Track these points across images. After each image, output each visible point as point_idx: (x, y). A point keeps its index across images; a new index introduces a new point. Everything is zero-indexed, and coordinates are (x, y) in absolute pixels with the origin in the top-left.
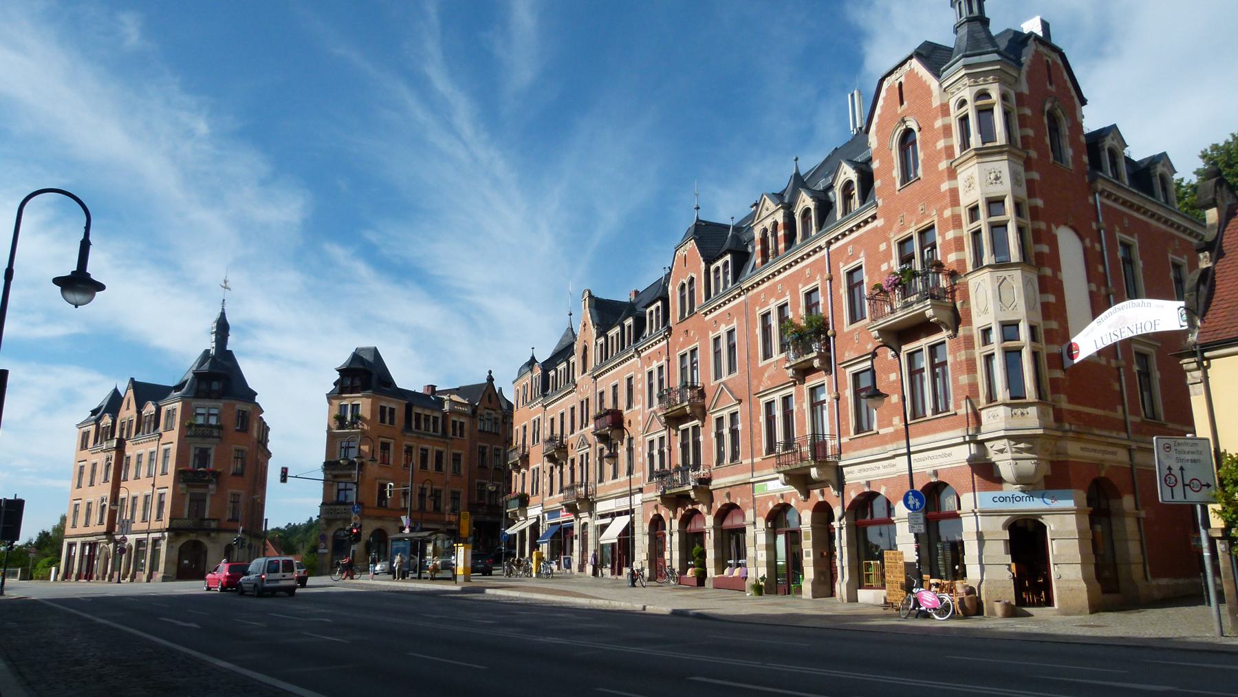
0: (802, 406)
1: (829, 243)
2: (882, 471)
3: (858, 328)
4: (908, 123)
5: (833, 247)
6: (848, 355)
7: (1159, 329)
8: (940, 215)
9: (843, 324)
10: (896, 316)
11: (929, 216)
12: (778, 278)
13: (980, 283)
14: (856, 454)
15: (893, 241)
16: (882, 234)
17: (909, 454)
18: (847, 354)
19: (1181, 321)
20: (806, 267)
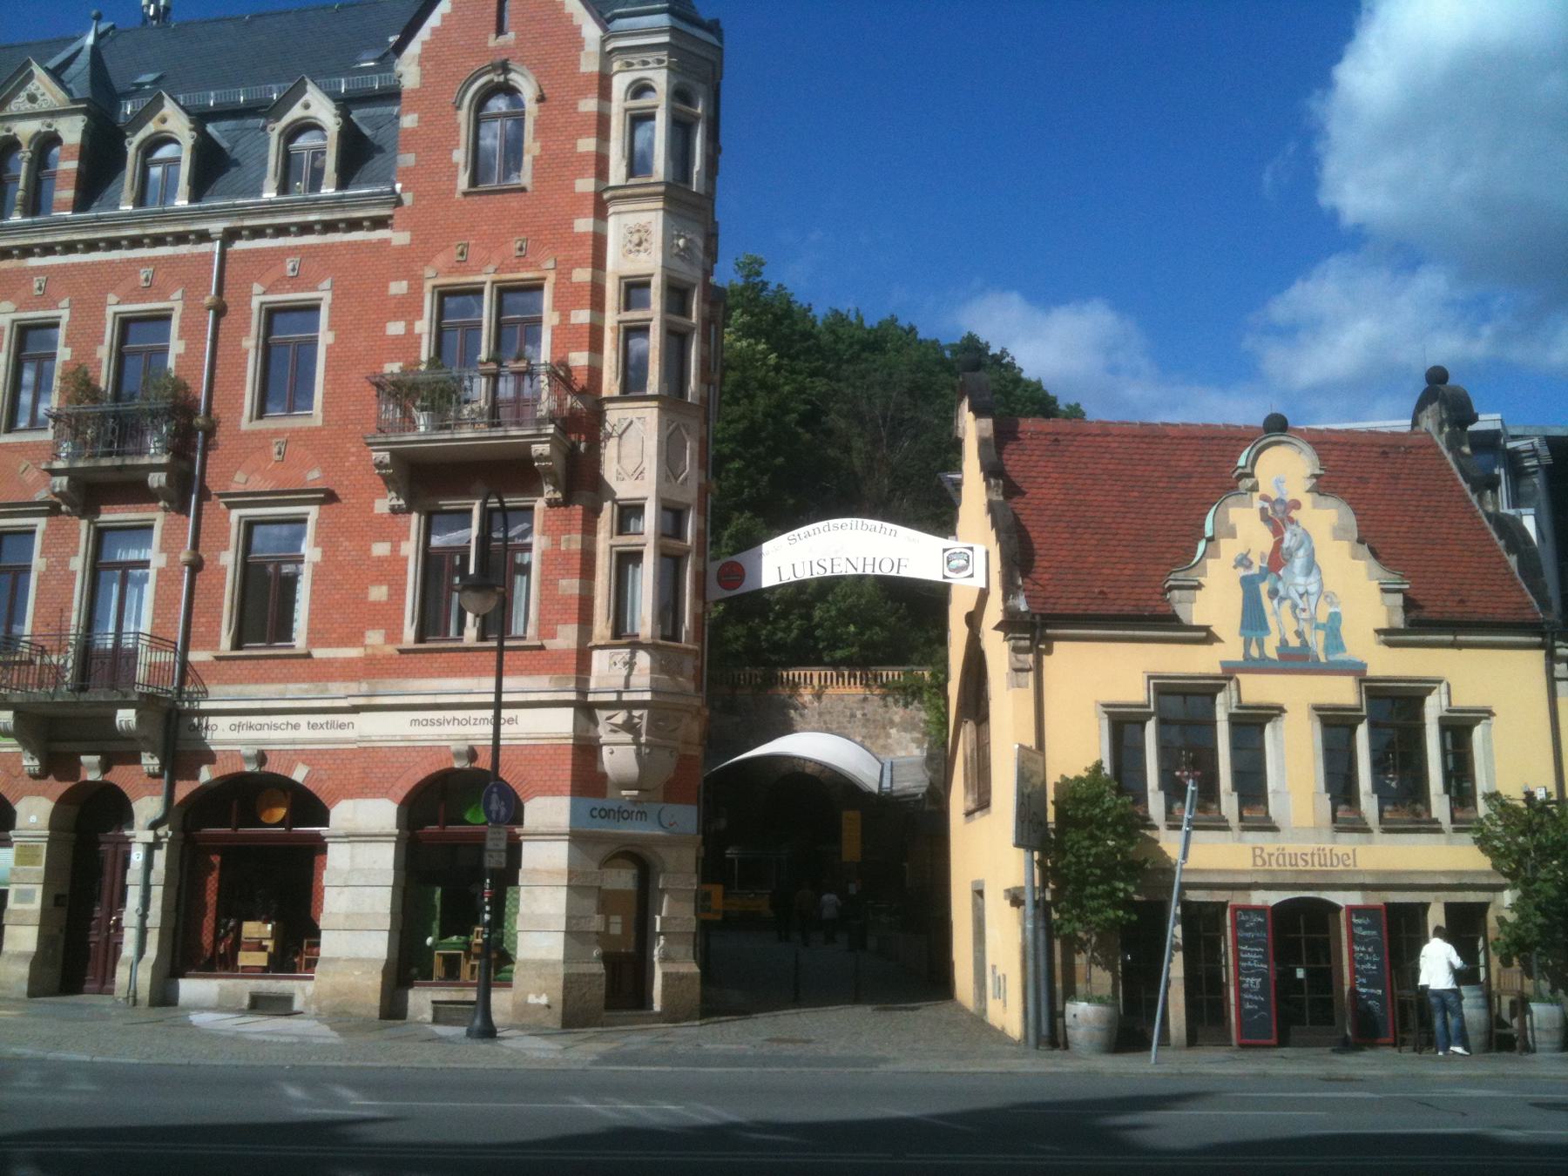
0: (65, 563)
1: (231, 236)
2: (305, 733)
3: (285, 431)
4: (512, 76)
5: (240, 245)
6: (240, 481)
7: (904, 573)
8: (563, 274)
9: (241, 414)
10: (457, 436)
11: (535, 265)
12: (34, 262)
13: (631, 423)
14: (234, 690)
15: (428, 285)
16: (406, 264)
17: (498, 706)
18: (240, 477)
19: (946, 569)
20: (143, 262)
